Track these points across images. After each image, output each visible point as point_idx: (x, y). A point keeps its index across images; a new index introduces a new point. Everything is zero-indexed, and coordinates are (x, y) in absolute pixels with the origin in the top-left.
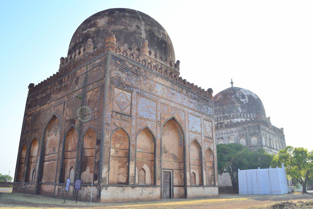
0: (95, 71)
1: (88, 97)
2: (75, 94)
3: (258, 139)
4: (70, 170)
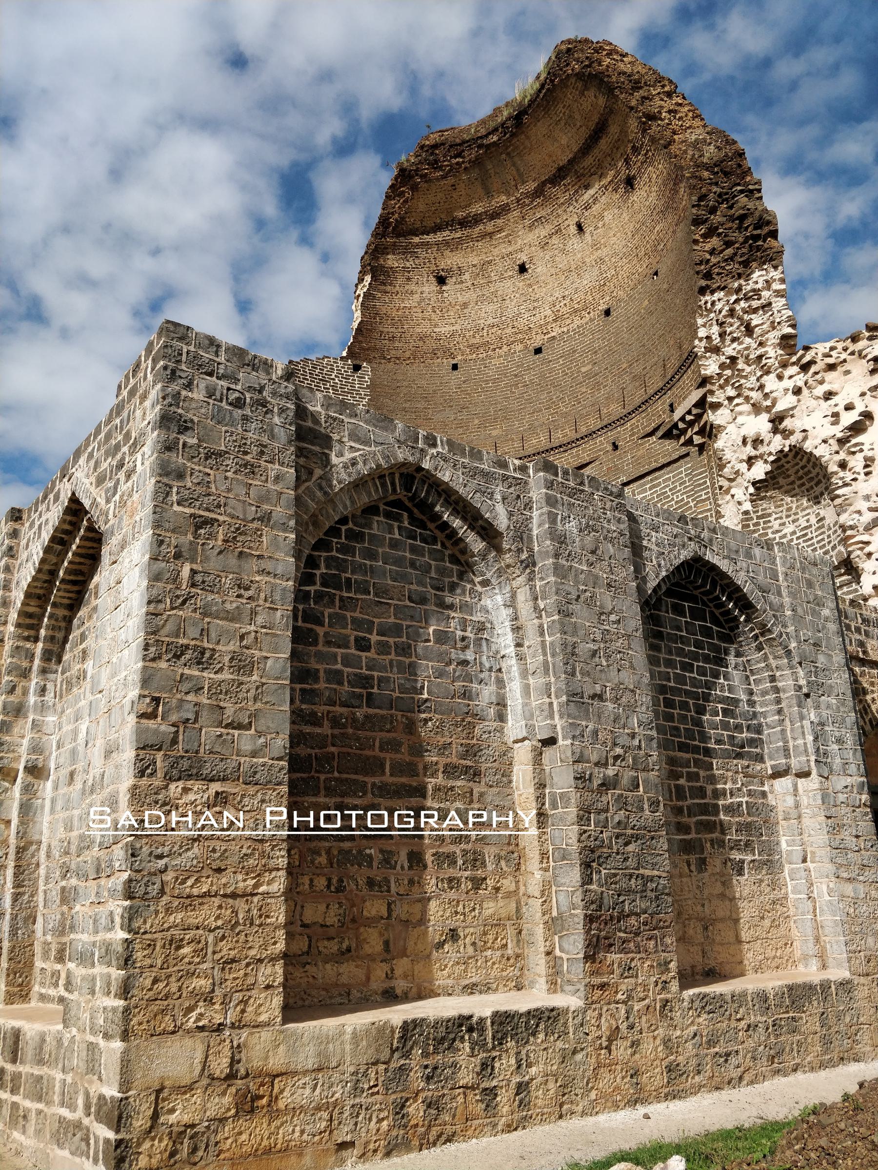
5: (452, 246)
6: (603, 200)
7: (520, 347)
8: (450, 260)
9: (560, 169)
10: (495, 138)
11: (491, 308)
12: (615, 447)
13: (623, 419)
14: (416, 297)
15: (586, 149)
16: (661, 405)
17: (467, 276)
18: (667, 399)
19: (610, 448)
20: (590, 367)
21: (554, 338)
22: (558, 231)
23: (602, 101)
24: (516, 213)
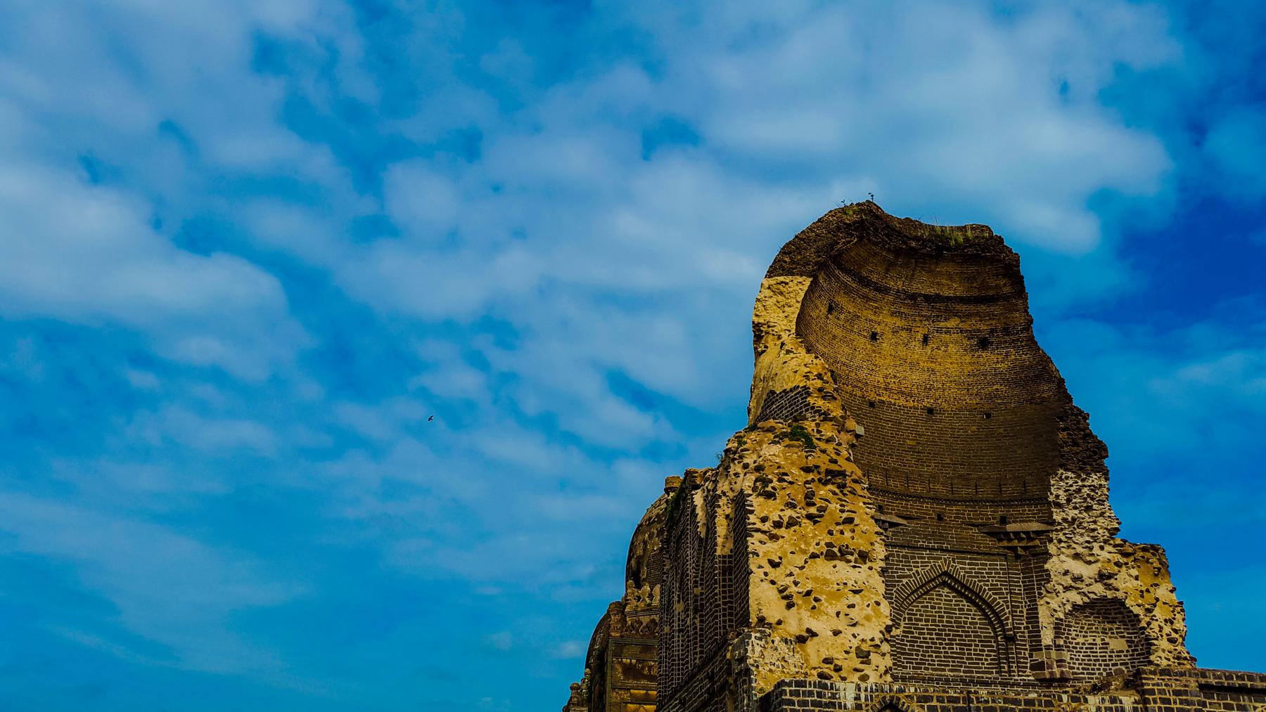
5: (848, 290)
7: (859, 394)
8: (842, 300)
10: (914, 244)
11: (847, 350)
12: (940, 518)
15: (961, 300)
17: (842, 317)
18: (1001, 511)
20: (914, 443)
21: (883, 402)
24: (891, 298)
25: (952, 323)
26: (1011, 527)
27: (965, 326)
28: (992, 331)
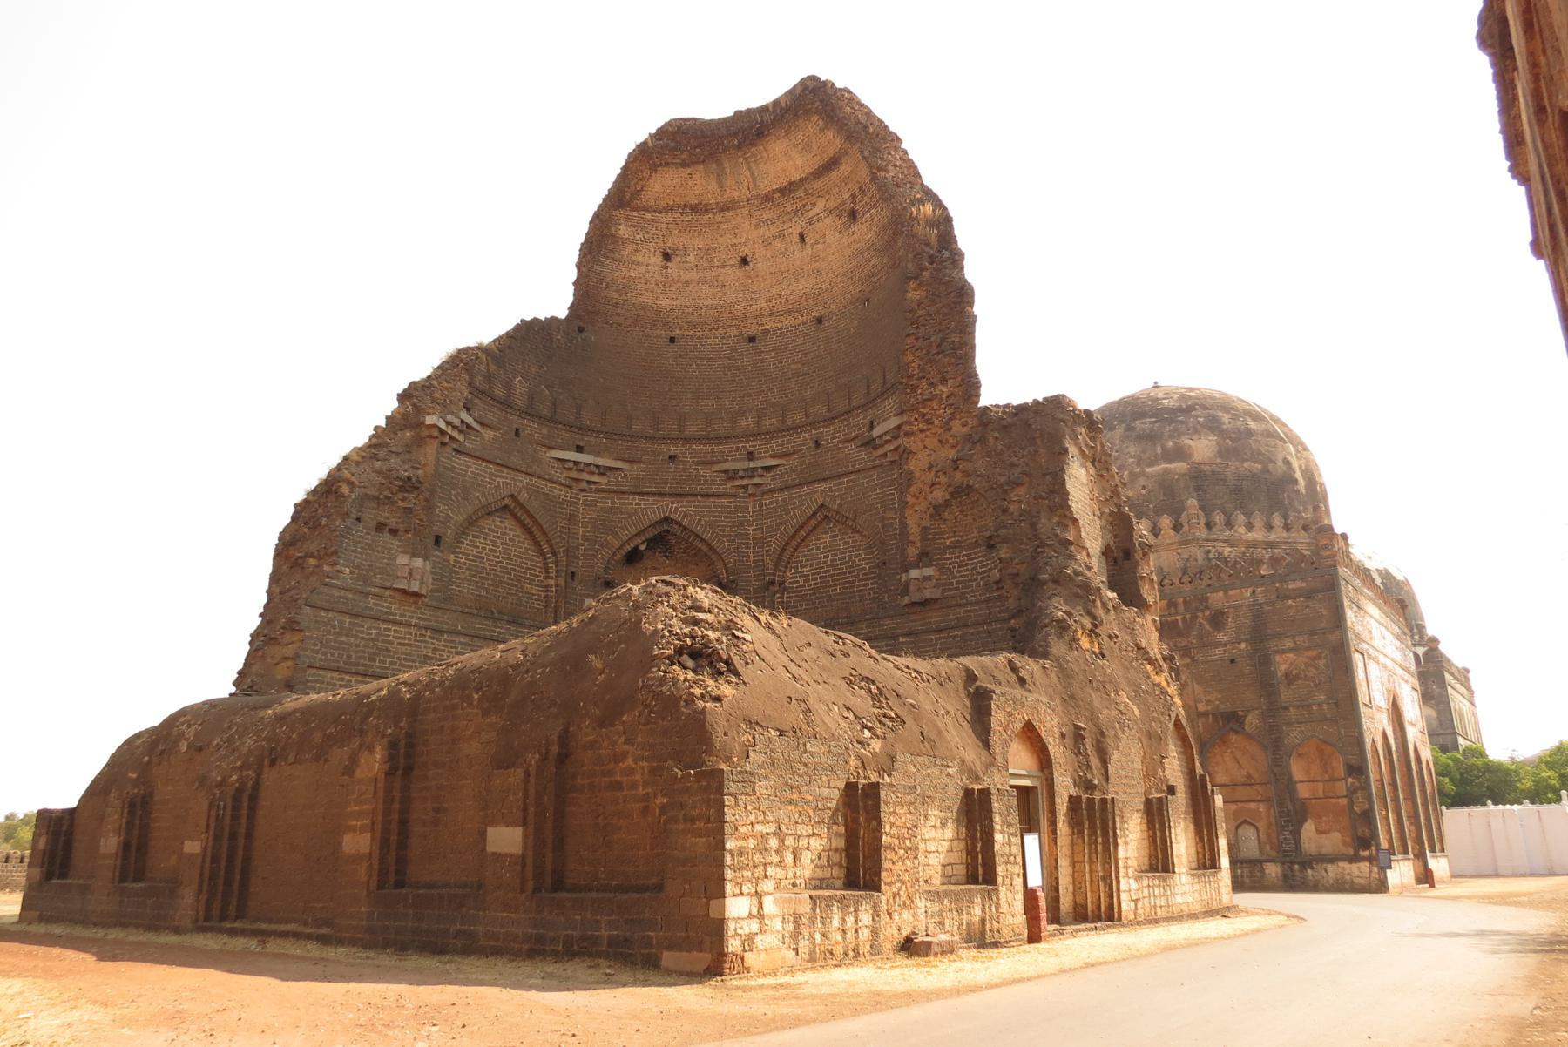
0: (1290, 607)
1: (1284, 667)
2: (1219, 654)
3: (1439, 712)
4: (1237, 828)
6: (827, 221)
9: (791, 183)
12: (817, 444)
13: (829, 420)
14: (642, 269)
16: (861, 420)
17: (692, 257)
19: (812, 444)
22: (782, 236)
23: (838, 142)
25: (820, 205)
26: (876, 432)
27: (832, 204)
28: (853, 196)
